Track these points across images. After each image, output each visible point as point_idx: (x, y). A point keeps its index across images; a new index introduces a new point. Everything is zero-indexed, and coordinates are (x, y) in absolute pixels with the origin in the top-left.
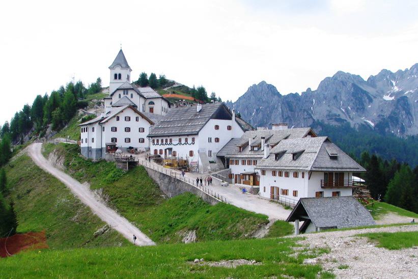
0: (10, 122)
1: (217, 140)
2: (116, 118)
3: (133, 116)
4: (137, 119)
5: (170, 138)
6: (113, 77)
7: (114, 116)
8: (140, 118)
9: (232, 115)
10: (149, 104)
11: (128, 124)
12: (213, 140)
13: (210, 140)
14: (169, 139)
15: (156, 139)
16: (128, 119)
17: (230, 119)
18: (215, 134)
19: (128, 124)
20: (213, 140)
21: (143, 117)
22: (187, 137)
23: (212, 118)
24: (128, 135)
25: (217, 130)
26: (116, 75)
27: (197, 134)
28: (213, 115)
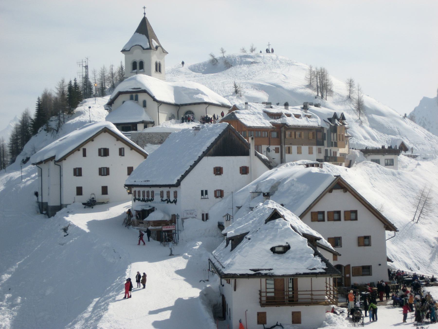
1: (219, 194)
2: (81, 152)
4: (121, 152)
7: (77, 149)
8: (127, 150)
9: (248, 146)
11: (104, 162)
12: (211, 194)
13: (204, 193)
16: (105, 152)
17: (246, 153)
19: (104, 162)
20: (211, 194)
21: (132, 148)
23: (206, 154)
24: (104, 181)
25: (218, 177)
27: (178, 184)
28: (209, 149)
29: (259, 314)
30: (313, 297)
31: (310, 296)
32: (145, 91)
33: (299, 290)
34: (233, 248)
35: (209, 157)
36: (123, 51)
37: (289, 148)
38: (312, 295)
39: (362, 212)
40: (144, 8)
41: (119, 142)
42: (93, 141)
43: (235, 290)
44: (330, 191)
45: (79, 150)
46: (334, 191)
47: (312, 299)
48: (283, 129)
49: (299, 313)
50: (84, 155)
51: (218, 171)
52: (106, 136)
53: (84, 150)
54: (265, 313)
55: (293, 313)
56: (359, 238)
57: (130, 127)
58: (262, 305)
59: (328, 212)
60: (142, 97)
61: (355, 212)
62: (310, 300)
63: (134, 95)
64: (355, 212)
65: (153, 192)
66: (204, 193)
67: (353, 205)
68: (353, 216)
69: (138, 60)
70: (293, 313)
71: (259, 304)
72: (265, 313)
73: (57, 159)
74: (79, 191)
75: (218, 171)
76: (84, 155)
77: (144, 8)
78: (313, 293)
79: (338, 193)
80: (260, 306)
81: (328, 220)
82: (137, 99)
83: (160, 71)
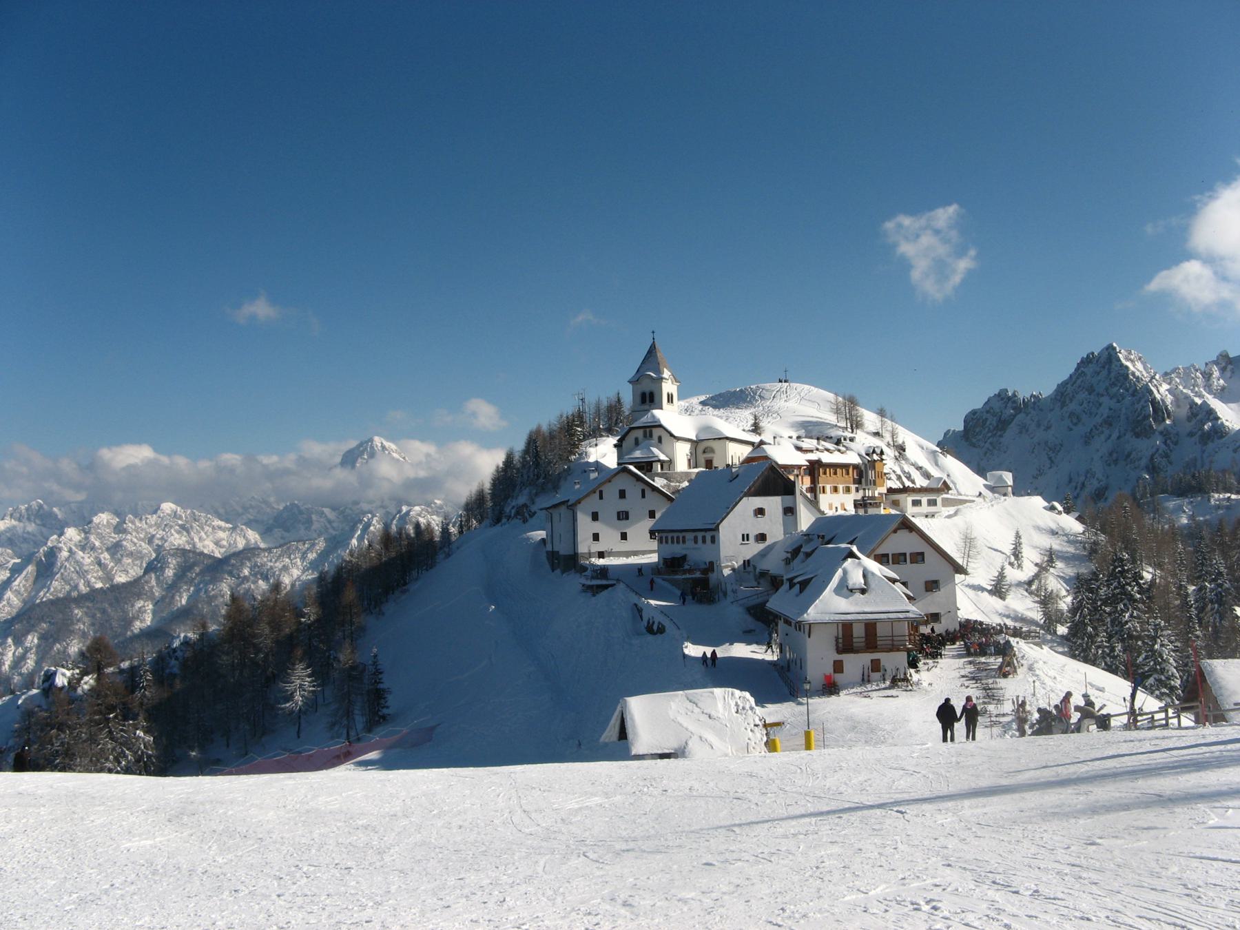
0: (487, 486)
1: (761, 537)
3: (633, 490)
5: (684, 534)
6: (639, 399)
8: (648, 492)
10: (704, 452)
11: (623, 505)
12: (752, 538)
13: (745, 537)
14: (681, 535)
15: (664, 535)
18: (761, 525)
20: (752, 538)
22: (703, 533)
26: (643, 395)
29: (835, 662)
30: (895, 643)
31: (891, 642)
32: (661, 426)
33: (878, 635)
34: (801, 591)
35: (750, 498)
36: (630, 382)
37: (823, 487)
38: (893, 640)
39: (929, 553)
40: (653, 332)
41: (639, 483)
42: (610, 481)
43: (809, 637)
44: (895, 531)
45: (595, 492)
46: (898, 531)
47: (893, 645)
48: (816, 466)
49: (879, 660)
50: (601, 498)
51: (760, 512)
52: (624, 476)
53: (601, 492)
54: (841, 662)
55: (872, 661)
56: (926, 583)
57: (643, 466)
58: (839, 651)
59: (893, 555)
60: (656, 432)
61: (922, 554)
62: (890, 647)
63: (648, 430)
64: (922, 554)
65: (684, 537)
66: (745, 537)
67: (920, 546)
68: (920, 558)
69: (647, 390)
70: (872, 661)
71: (835, 652)
72: (841, 662)
73: (570, 503)
74: (596, 537)
75: (760, 512)
76: (601, 498)
77: (653, 332)
78: (895, 638)
79: (903, 534)
80: (836, 654)
81: (893, 563)
82: (651, 436)
83: (672, 402)
